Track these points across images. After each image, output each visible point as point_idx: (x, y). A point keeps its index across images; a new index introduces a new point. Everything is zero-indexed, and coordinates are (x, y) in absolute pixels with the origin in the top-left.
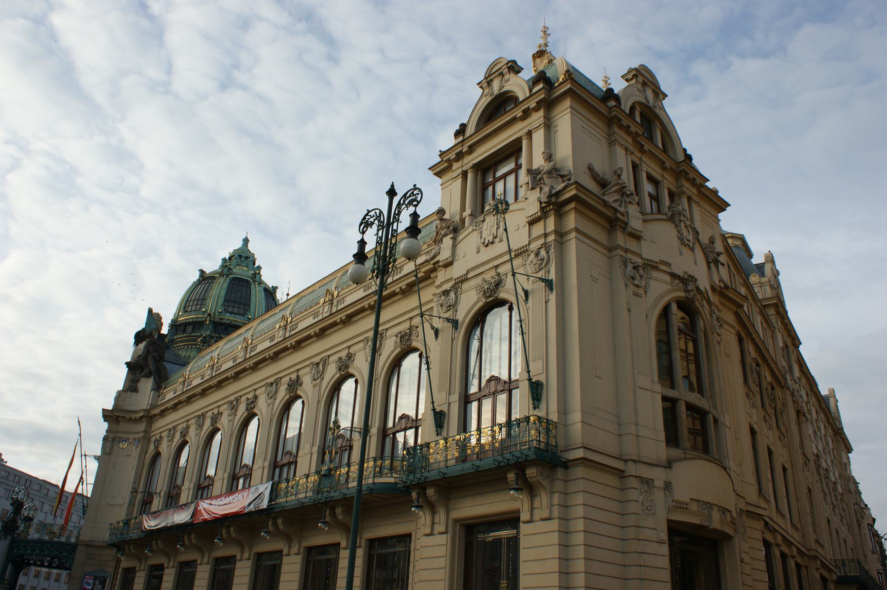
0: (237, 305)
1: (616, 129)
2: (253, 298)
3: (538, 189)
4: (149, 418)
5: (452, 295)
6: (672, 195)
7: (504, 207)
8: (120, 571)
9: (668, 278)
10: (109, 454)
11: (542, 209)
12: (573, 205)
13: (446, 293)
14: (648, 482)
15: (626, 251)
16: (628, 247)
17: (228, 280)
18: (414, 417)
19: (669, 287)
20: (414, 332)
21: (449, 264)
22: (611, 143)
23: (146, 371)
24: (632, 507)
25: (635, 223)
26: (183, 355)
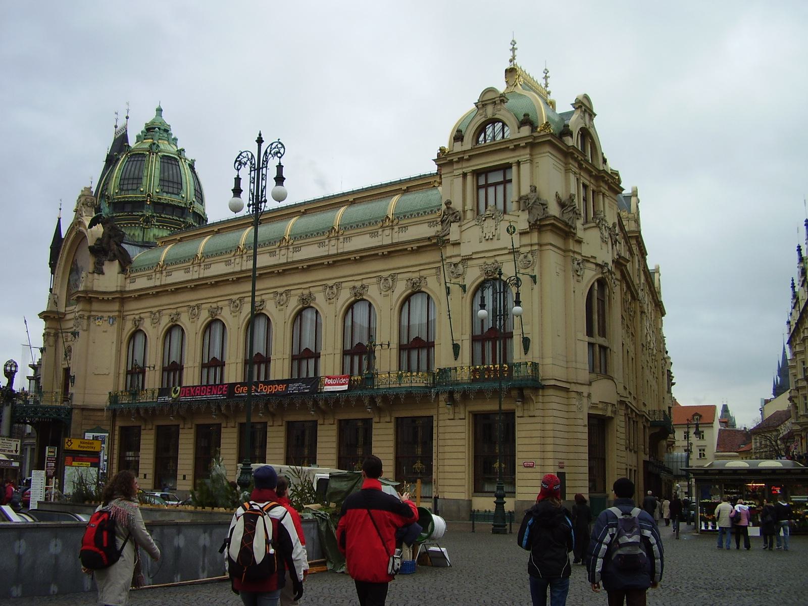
0: (171, 185)
1: (571, 161)
2: (183, 176)
3: (527, 211)
4: (122, 298)
5: (460, 266)
6: (594, 192)
7: (513, 230)
8: (117, 428)
9: (593, 266)
10: (87, 330)
11: (530, 226)
12: (549, 228)
13: (456, 265)
14: (580, 394)
15: (574, 252)
16: (576, 250)
17: (158, 159)
18: (425, 340)
19: (594, 273)
20: (423, 281)
21: (457, 244)
22: (567, 170)
23: (111, 254)
24: (574, 408)
25: (580, 233)
26: (127, 233)
